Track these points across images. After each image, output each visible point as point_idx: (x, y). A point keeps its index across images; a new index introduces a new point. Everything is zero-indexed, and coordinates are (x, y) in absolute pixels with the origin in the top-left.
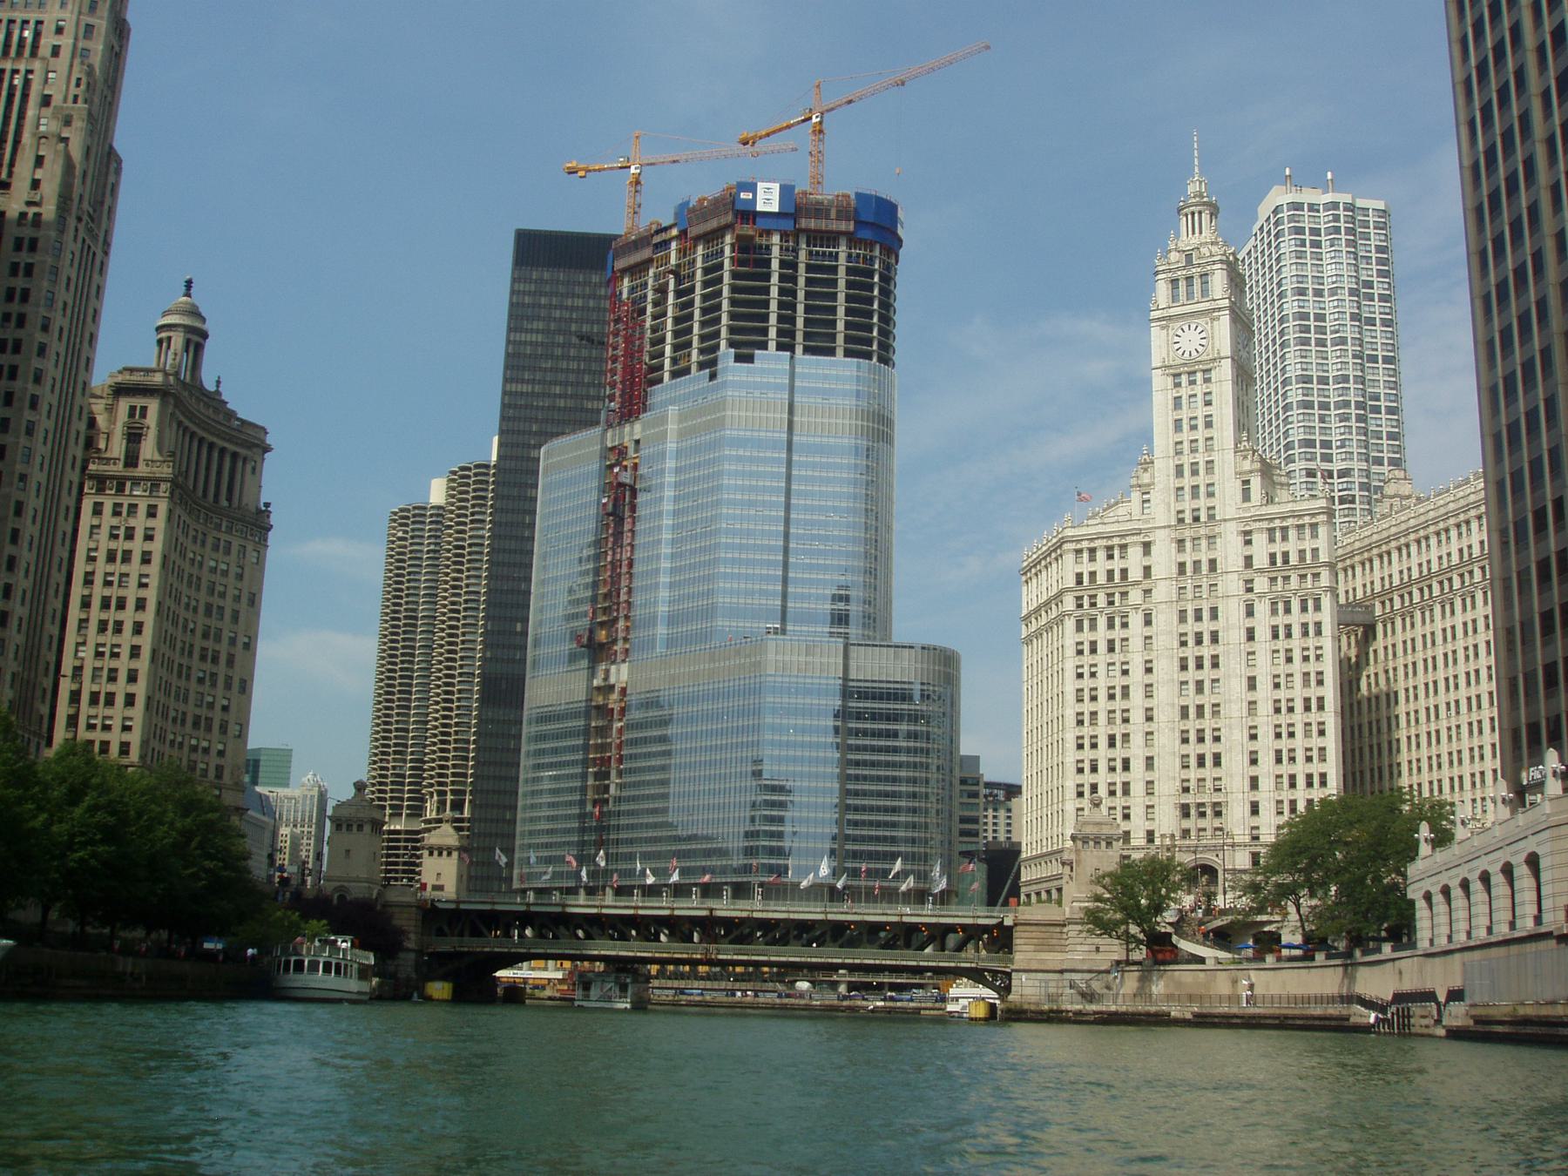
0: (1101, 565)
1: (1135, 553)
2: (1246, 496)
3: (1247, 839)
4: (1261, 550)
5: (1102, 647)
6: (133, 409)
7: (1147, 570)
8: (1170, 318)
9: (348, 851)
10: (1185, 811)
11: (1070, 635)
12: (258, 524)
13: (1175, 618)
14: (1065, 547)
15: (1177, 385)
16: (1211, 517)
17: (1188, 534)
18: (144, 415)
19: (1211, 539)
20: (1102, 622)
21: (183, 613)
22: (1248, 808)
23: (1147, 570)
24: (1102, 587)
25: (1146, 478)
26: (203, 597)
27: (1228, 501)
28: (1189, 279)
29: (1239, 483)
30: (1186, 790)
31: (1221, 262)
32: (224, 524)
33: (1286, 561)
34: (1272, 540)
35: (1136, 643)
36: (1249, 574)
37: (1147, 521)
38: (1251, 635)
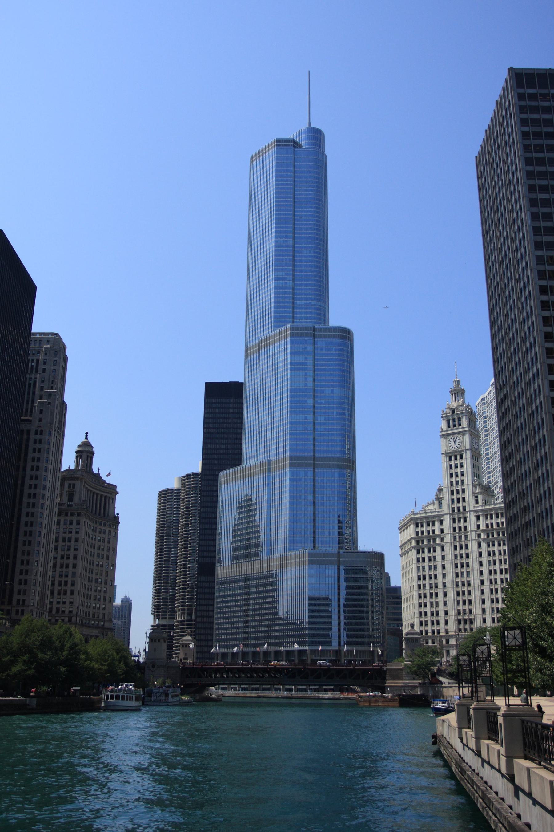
1: (437, 524)
2: (477, 502)
4: (482, 522)
6: (70, 485)
7: (442, 531)
9: (155, 649)
10: (459, 622)
12: (116, 521)
15: (450, 459)
18: (74, 487)
20: (426, 550)
21: (89, 558)
26: (96, 551)
27: (470, 505)
29: (474, 497)
30: (459, 613)
35: (439, 558)
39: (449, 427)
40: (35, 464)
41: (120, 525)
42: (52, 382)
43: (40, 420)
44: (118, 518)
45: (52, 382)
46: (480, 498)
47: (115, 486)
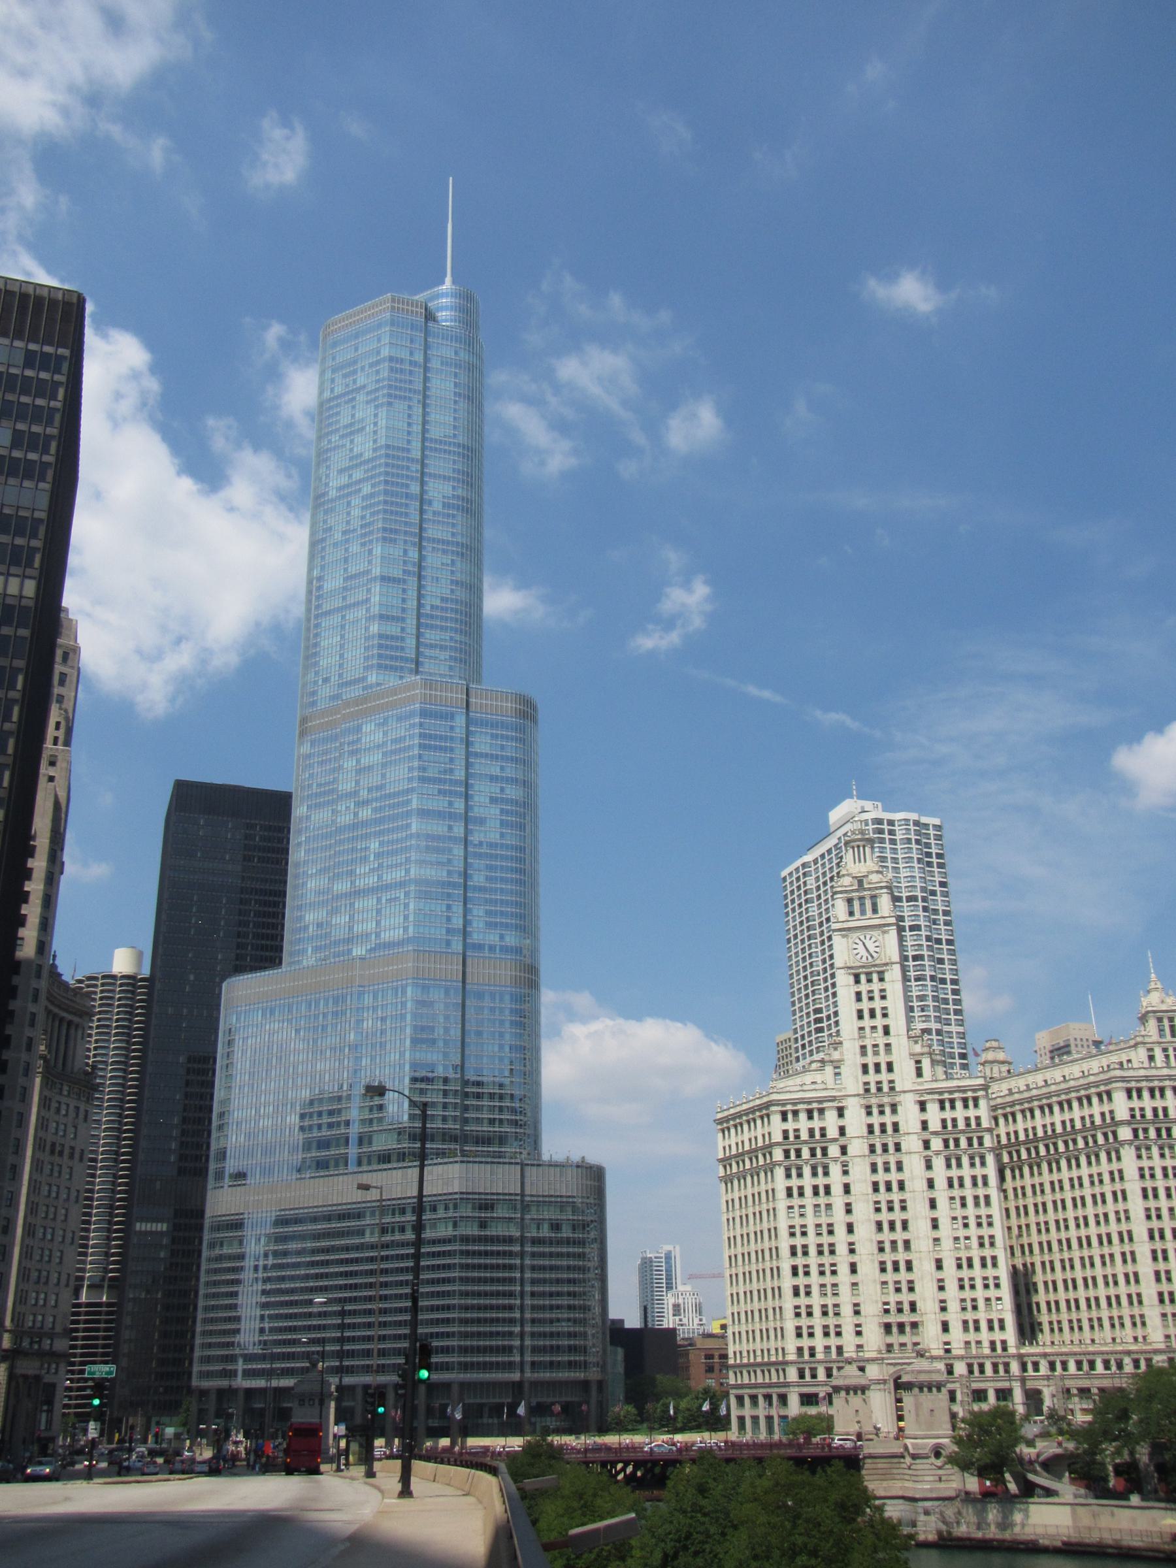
0: (803, 1124)
1: (831, 1117)
2: (919, 1073)
3: (941, 1352)
4: (934, 1115)
5: (808, 1191)
7: (842, 1131)
8: (849, 929)
10: (887, 1327)
11: (780, 1181)
13: (868, 1169)
14: (773, 1108)
15: (857, 981)
16: (892, 1089)
17: (874, 1101)
19: (894, 1108)
20: (807, 1171)
22: (939, 1327)
23: (842, 1131)
24: (805, 1142)
25: (836, 1055)
27: (904, 1075)
28: (861, 898)
29: (912, 1063)
30: (887, 1311)
31: (886, 887)
32: (66, 1088)
33: (955, 1125)
34: (942, 1108)
36: (926, 1135)
37: (840, 1090)
38: (931, 1184)
39: (851, 914)
46: (926, 1064)
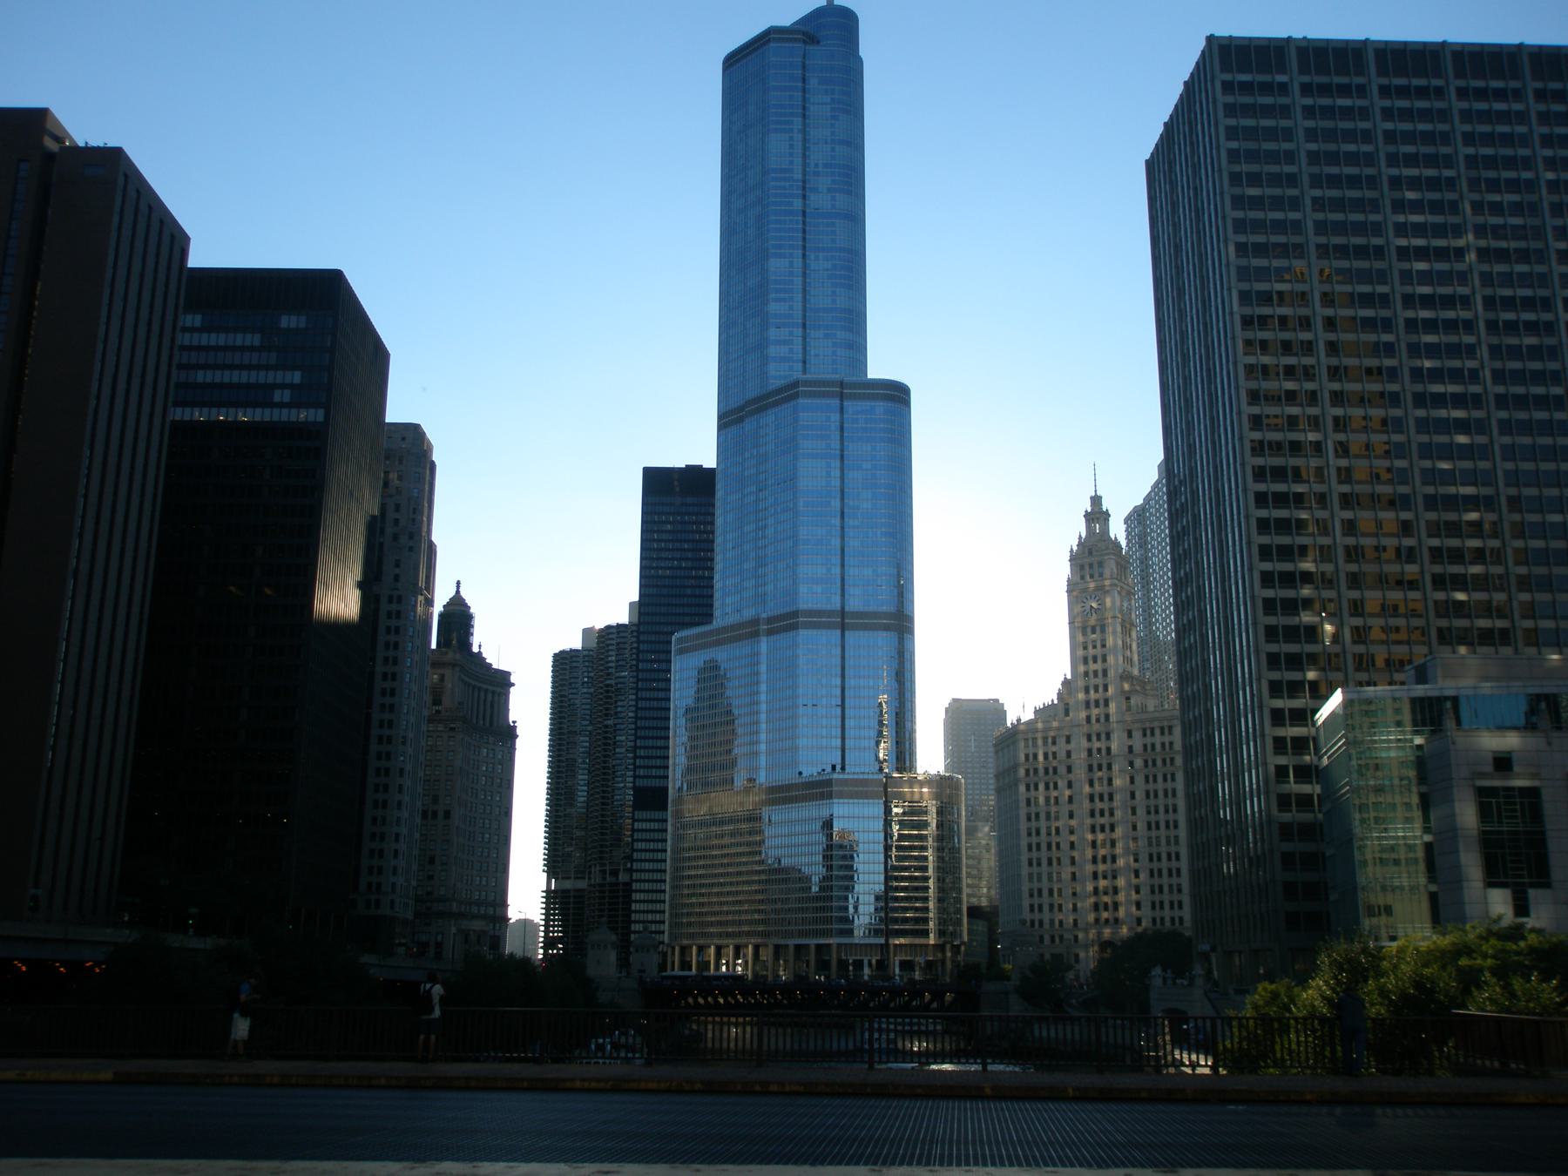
1: (1062, 741)
23: (1069, 754)
40: (391, 653)
41: (518, 741)
42: (414, 513)
43: (397, 578)
44: (514, 728)
45: (414, 513)
47: (508, 674)
